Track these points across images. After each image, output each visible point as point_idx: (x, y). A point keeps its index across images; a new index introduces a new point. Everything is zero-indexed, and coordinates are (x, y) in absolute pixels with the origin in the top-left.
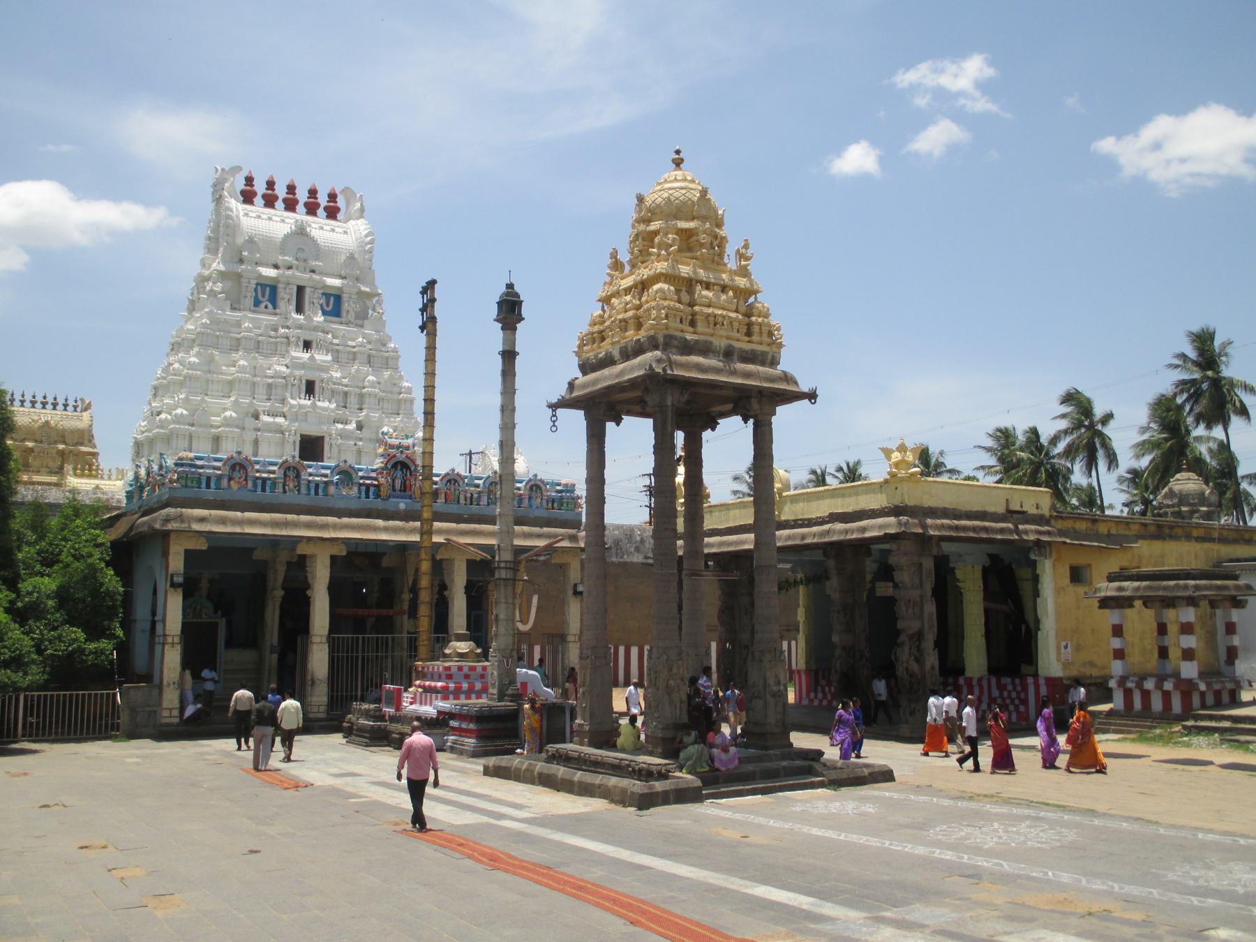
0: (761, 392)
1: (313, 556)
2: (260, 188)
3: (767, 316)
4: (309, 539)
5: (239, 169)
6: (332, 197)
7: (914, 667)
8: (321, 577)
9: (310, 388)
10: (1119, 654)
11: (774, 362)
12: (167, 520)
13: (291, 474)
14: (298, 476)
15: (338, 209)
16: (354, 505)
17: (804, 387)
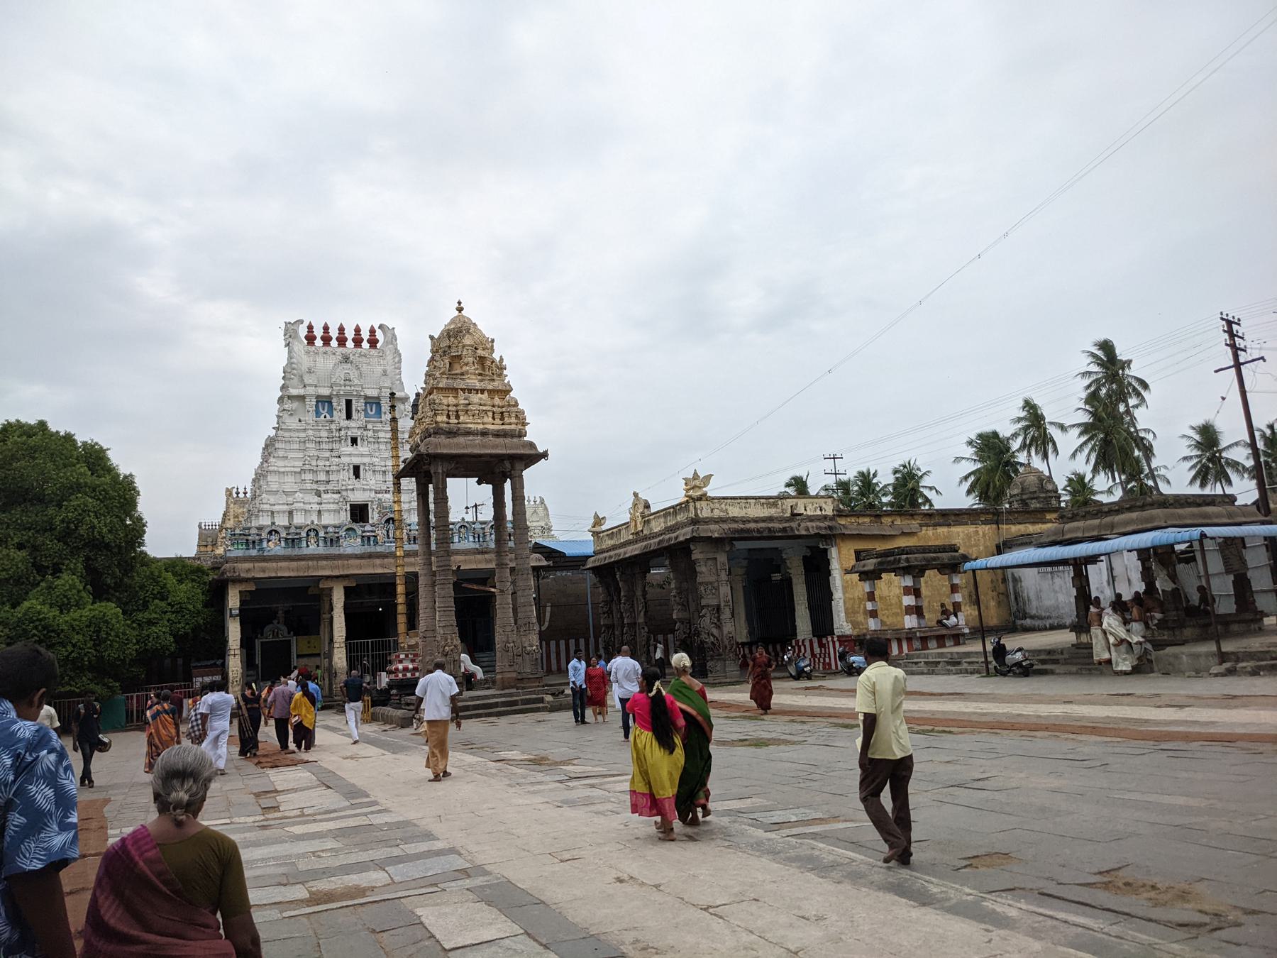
0: (501, 458)
1: (331, 589)
2: (318, 332)
3: (516, 404)
4: (328, 577)
5: (302, 322)
6: (372, 331)
7: (715, 631)
8: (338, 599)
9: (356, 470)
10: (873, 614)
11: (521, 434)
12: (223, 573)
13: (312, 534)
14: (317, 534)
15: (377, 341)
16: (358, 551)
17: (541, 450)
